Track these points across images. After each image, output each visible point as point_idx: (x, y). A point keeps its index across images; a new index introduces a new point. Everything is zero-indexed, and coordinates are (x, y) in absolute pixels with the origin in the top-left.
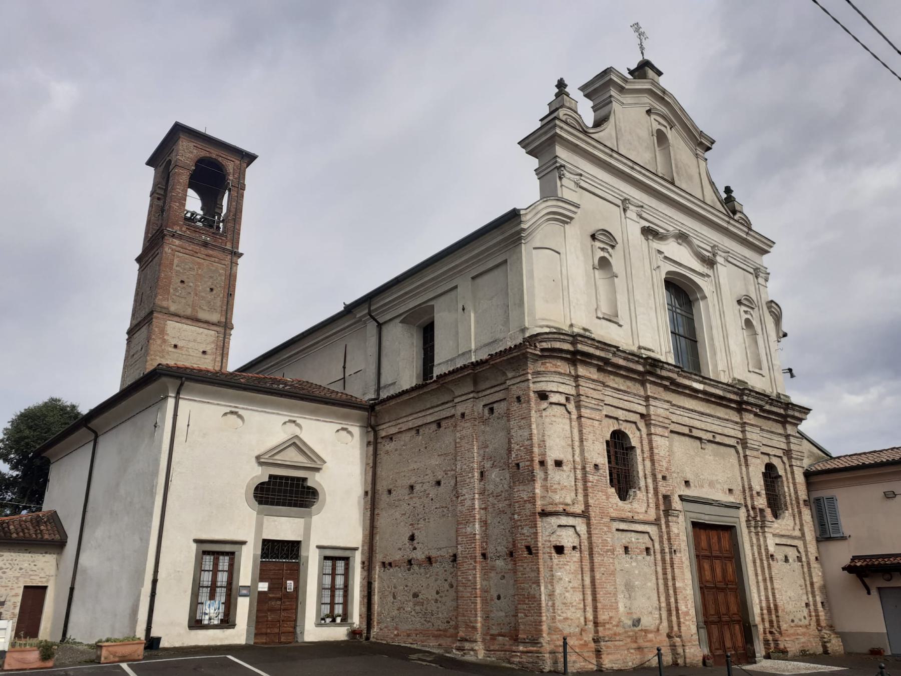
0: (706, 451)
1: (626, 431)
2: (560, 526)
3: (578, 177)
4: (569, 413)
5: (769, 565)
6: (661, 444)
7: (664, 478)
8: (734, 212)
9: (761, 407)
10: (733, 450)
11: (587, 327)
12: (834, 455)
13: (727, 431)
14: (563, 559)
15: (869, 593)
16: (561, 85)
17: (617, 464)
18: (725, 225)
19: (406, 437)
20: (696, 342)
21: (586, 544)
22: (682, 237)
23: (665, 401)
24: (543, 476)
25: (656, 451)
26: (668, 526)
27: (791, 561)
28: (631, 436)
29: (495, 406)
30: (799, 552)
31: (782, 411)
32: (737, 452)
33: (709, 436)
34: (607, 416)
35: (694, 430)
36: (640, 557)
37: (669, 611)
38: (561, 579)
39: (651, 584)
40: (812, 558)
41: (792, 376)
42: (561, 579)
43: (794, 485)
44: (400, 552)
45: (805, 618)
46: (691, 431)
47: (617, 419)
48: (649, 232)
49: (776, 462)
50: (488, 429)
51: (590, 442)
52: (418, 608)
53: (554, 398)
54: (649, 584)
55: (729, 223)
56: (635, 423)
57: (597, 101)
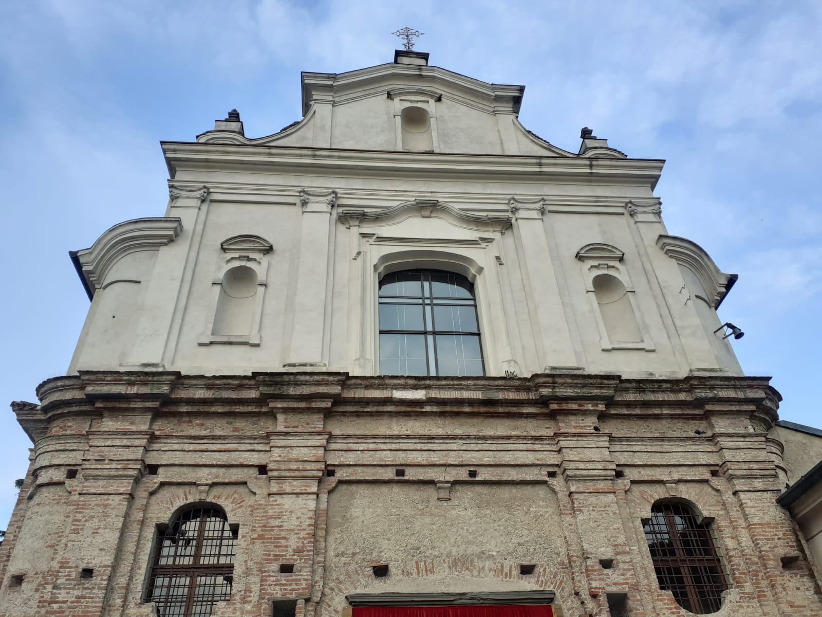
13: (508, 458)
18: (536, 169)
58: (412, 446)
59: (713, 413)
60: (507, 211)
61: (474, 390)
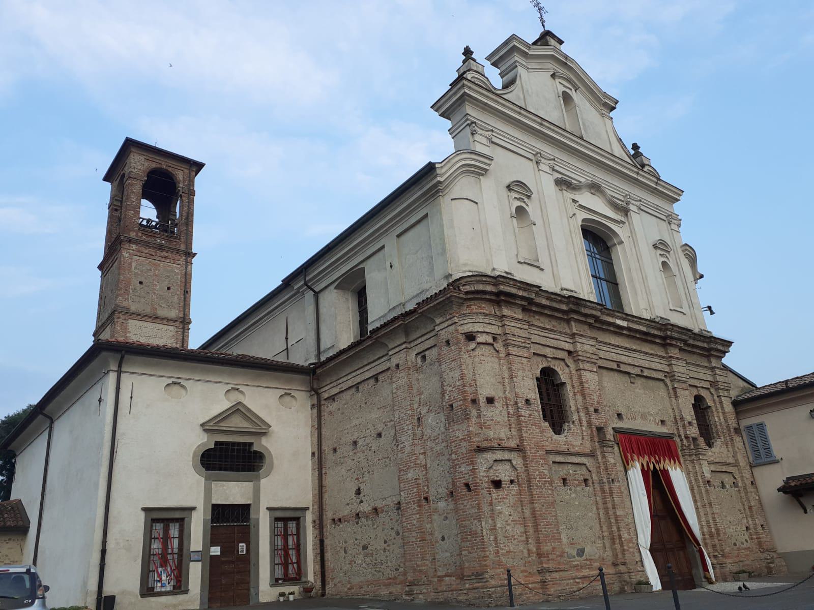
0: (636, 385)
1: (556, 368)
2: (496, 461)
3: (490, 133)
4: (497, 351)
5: (707, 490)
6: (591, 378)
7: (596, 411)
8: (643, 166)
9: (685, 342)
10: (661, 384)
11: (507, 271)
12: (758, 386)
13: (653, 366)
14: (501, 493)
15: (806, 512)
16: (468, 52)
17: (549, 400)
19: (347, 396)
20: (617, 284)
21: (524, 476)
22: (595, 188)
23: (591, 338)
24: (476, 414)
25: (586, 385)
26: (604, 457)
27: (728, 486)
28: (560, 373)
29: (427, 353)
30: (735, 478)
31: (705, 345)
32: (666, 385)
33: (637, 371)
34: (534, 354)
35: (621, 365)
36: (578, 489)
37: (613, 539)
38: (501, 513)
39: (592, 514)
40: (748, 483)
41: (712, 313)
42: (501, 513)
43: (722, 414)
44: (348, 507)
45: (746, 541)
46: (618, 366)
47: (545, 356)
48: (563, 183)
49: (704, 393)
50: (421, 376)
51: (520, 378)
52: (368, 559)
53: (481, 338)
54: (590, 514)
55: (638, 173)
56: (563, 360)
57: (504, 68)
58: (622, 353)
59: (671, 345)
60: (623, 201)
61: (644, 326)
